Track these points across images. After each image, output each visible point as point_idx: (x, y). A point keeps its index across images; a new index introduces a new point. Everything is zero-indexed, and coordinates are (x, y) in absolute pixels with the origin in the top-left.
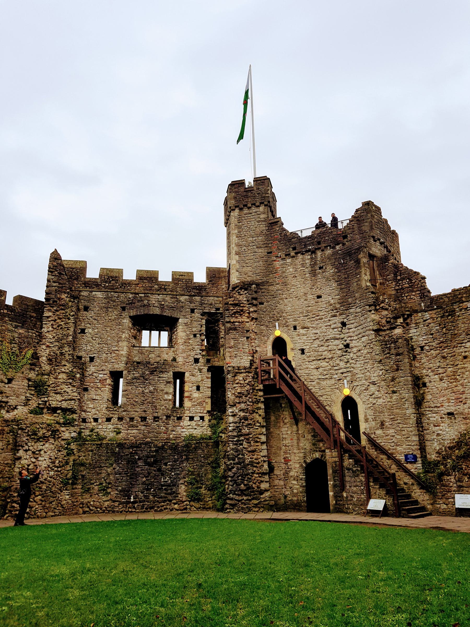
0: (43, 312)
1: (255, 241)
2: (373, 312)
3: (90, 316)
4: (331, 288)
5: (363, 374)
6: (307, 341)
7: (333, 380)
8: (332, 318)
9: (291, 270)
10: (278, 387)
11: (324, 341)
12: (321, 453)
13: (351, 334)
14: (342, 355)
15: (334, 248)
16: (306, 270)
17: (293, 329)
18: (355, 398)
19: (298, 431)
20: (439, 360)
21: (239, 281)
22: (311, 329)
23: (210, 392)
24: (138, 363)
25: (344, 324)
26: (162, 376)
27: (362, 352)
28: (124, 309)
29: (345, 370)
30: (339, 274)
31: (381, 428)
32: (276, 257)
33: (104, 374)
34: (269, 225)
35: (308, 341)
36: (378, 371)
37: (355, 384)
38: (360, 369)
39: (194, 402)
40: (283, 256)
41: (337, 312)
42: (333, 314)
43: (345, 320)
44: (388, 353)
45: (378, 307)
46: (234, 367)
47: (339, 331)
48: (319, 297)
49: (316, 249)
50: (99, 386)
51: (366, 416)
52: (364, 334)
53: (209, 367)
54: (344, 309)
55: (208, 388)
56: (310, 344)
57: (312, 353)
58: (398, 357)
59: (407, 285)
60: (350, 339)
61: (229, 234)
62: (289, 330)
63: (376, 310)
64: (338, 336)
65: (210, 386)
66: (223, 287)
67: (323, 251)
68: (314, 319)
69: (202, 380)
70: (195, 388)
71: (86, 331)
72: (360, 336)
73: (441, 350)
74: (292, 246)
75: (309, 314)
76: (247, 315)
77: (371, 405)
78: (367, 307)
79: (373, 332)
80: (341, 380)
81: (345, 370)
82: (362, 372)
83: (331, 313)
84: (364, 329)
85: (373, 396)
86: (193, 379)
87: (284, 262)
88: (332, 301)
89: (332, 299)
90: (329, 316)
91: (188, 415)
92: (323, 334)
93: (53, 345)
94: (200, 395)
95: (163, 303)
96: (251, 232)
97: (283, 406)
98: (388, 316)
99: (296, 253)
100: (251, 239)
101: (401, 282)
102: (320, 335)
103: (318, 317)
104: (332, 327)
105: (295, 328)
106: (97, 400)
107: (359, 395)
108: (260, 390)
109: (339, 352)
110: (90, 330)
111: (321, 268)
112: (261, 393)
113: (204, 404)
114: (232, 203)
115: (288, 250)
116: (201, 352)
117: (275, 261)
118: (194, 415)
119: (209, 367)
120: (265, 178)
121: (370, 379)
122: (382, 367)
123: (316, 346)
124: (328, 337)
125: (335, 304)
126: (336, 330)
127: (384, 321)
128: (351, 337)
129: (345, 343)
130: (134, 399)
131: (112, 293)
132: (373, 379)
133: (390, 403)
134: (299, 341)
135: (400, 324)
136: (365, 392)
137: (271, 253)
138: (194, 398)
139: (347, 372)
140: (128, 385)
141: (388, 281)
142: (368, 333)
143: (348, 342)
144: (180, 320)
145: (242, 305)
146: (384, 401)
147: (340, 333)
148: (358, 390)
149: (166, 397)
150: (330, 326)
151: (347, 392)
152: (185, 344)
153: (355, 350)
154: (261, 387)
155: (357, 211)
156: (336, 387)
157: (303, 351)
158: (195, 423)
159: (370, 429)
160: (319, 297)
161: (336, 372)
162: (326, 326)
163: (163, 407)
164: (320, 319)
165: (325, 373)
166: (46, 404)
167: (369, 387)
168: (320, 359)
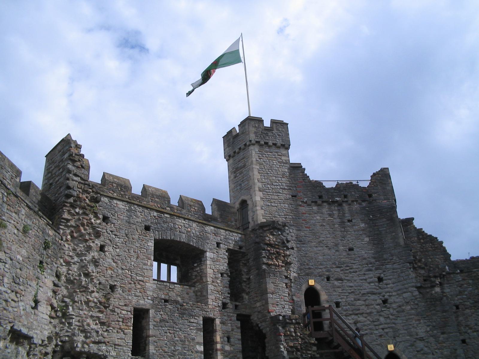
1: (278, 181)
2: (412, 269)
3: (111, 229)
4: (363, 243)
5: (406, 330)
6: (342, 294)
7: (374, 335)
8: (367, 273)
9: (318, 217)
11: (360, 295)
14: (382, 311)
15: (360, 204)
16: (335, 220)
17: (326, 280)
20: (476, 318)
21: (265, 220)
23: (241, 346)
24: (166, 301)
25: (380, 280)
26: (192, 320)
27: (404, 308)
28: (147, 228)
29: (386, 326)
32: (302, 202)
33: (127, 311)
34: (291, 168)
36: (426, 327)
37: (398, 339)
38: (402, 325)
41: (372, 267)
42: (368, 268)
43: (382, 275)
44: (434, 310)
46: (284, 316)
47: (377, 286)
49: (343, 201)
50: (122, 327)
52: (405, 290)
54: (379, 264)
55: (239, 340)
56: (345, 297)
57: (349, 307)
58: (444, 314)
60: (388, 294)
62: (323, 280)
63: (414, 268)
64: (375, 291)
65: (240, 337)
68: (347, 272)
69: (233, 330)
70: (226, 339)
71: (106, 249)
73: (476, 309)
74: (319, 194)
76: (282, 258)
78: (408, 264)
80: (383, 336)
81: (386, 325)
82: (405, 328)
83: (366, 266)
84: (406, 286)
85: (422, 352)
87: (311, 208)
88: (366, 255)
89: (366, 253)
90: (364, 269)
92: (359, 288)
93: (72, 261)
94: (232, 349)
95: (189, 229)
96: (274, 171)
98: (425, 275)
99: (323, 202)
100: (274, 178)
101: (425, 245)
102: (356, 288)
103: (352, 270)
104: (368, 280)
105: (328, 279)
106: (120, 346)
108: (314, 344)
109: (378, 307)
110: (111, 249)
111: (349, 221)
112: (315, 348)
115: (314, 197)
117: (300, 206)
120: (282, 122)
121: (417, 335)
122: (429, 323)
123: (352, 299)
126: (372, 284)
127: (422, 279)
128: (389, 292)
129: (383, 299)
130: (164, 348)
131: (136, 206)
135: (438, 283)
136: (409, 348)
137: (295, 196)
139: (389, 327)
142: (410, 289)
143: (386, 297)
144: (208, 254)
145: (277, 247)
147: (378, 288)
150: (366, 280)
151: (391, 347)
152: (213, 284)
153: (394, 305)
154: (313, 341)
156: (378, 343)
160: (351, 249)
161: (377, 327)
162: (361, 280)
164: (354, 272)
167: (415, 343)
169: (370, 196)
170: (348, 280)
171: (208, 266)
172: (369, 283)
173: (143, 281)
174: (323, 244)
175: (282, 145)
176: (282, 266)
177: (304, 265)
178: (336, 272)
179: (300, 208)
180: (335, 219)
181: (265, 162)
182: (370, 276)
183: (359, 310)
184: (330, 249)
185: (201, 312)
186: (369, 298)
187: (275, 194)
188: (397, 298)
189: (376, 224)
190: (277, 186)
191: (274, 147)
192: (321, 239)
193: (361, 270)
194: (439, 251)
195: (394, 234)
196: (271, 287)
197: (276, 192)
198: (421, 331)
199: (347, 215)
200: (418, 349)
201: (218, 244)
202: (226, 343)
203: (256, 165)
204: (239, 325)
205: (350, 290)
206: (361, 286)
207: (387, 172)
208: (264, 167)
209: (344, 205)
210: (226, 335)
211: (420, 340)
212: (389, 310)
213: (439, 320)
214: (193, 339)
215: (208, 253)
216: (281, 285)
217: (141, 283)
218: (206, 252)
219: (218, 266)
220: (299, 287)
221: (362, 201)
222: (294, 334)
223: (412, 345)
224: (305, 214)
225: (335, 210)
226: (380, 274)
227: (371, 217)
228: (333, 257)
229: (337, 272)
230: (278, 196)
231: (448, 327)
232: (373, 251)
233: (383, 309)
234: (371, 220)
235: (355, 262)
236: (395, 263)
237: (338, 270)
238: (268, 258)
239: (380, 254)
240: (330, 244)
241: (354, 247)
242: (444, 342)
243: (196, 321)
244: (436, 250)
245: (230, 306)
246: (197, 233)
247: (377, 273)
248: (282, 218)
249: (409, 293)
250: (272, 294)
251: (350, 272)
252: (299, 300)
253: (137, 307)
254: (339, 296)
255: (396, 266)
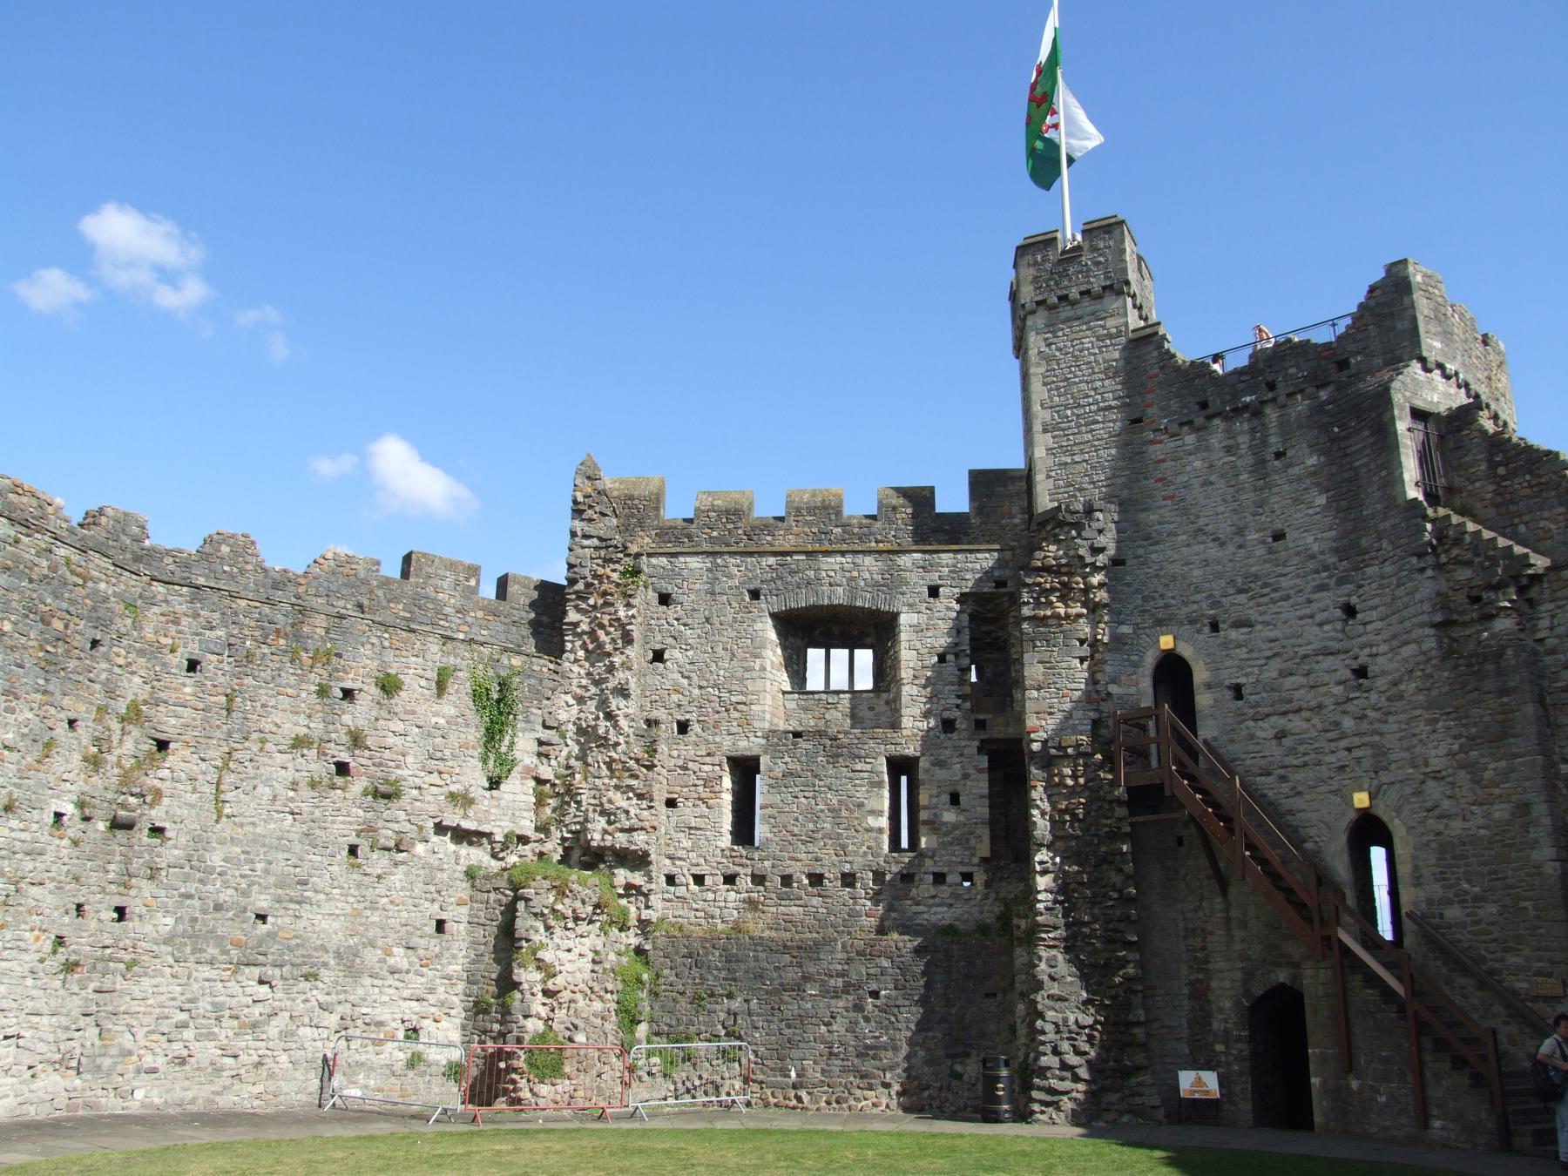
0: (565, 613)
1: (1093, 393)
2: (1430, 573)
4: (1311, 511)
5: (1407, 749)
8: (1316, 596)
9: (1198, 464)
10: (1167, 793)
11: (1297, 661)
12: (1291, 971)
13: (1371, 637)
14: (1349, 700)
17: (1207, 629)
18: (1385, 819)
19: (1227, 910)
22: (1259, 627)
24: (797, 735)
25: (1350, 611)
26: (858, 767)
29: (1356, 741)
30: (1334, 469)
31: (1459, 902)
35: (1253, 663)
36: (1450, 741)
37: (1384, 777)
39: (945, 835)
40: (1174, 428)
41: (1330, 577)
43: (1354, 600)
44: (1477, 689)
45: (1443, 559)
47: (1338, 631)
48: (1279, 536)
49: (1263, 403)
51: (1416, 868)
52: (1405, 636)
53: (982, 742)
55: (981, 797)
56: (1256, 670)
57: (1264, 695)
58: (1505, 700)
59: (1528, 491)
60: (1367, 651)
61: (1025, 377)
62: (1198, 631)
63: (1439, 567)
64: (1335, 645)
65: (986, 791)
66: (1017, 521)
67: (1283, 407)
68: (1265, 600)
69: (966, 776)
70: (946, 798)
71: (666, 656)
72: (1395, 643)
75: (1253, 586)
77: (1432, 837)
78: (1414, 560)
79: (1432, 631)
80: (1348, 770)
82: (1405, 744)
83: (1313, 579)
84: (1407, 624)
85: (1436, 812)
86: (940, 774)
87: (1180, 443)
88: (1315, 548)
91: (931, 870)
93: (588, 694)
94: (961, 818)
95: (855, 574)
97: (1186, 841)
99: (1209, 418)
100: (1084, 386)
101: (1508, 483)
102: (1285, 642)
103: (1276, 595)
104: (1318, 619)
105: (1215, 627)
107: (1398, 810)
108: (1119, 802)
109: (1338, 690)
111: (1279, 455)
112: (1121, 812)
113: (973, 842)
114: (1028, 294)
115: (1185, 411)
116: (959, 701)
117: (1152, 442)
118: (945, 870)
119: (982, 742)
120: (1113, 220)
121: (1427, 765)
123: (1274, 674)
124: (1308, 650)
125: (1322, 553)
126: (1327, 627)
127: (1460, 597)
128: (1371, 646)
130: (790, 828)
132: (1436, 763)
133: (1482, 832)
134: (1228, 664)
136: (1413, 799)
137: (1139, 420)
138: (945, 824)
139: (1364, 745)
140: (772, 790)
141: (1472, 483)
146: (1467, 825)
147: (1340, 636)
148: (1392, 795)
149: (872, 821)
150: (1311, 616)
151: (1361, 799)
152: (916, 682)
153: (1381, 683)
155: (1372, 289)
156: (1333, 788)
157: (1238, 691)
158: (949, 890)
159: (1429, 902)
160: (1279, 536)
162: (1301, 618)
163: (864, 848)
165: (1301, 749)
166: (578, 839)
167: (1424, 787)
168: (1285, 713)
169: (1343, 365)
170: (1267, 624)
171: (904, 645)
172: (1321, 625)
173: (745, 704)
174: (1205, 534)
175: (1104, 288)
176: (1079, 616)
177: (1154, 599)
178: (1234, 604)
179: (1151, 448)
180: (1241, 457)
181: (1060, 350)
182: (1321, 605)
183: (1291, 701)
184: (1222, 544)
185: (882, 747)
186: (1317, 667)
187: (1084, 428)
188: (1391, 660)
189: (1348, 451)
190: (1089, 405)
191: (1086, 302)
192: (1201, 522)
193: (1300, 591)
194: (1553, 493)
195: (1383, 473)
196: (1033, 670)
197: (1086, 424)
198: (1437, 756)
199: (1272, 439)
200: (1428, 805)
201: (934, 592)
202: (948, 806)
203: (1038, 365)
204: (986, 765)
205: (1271, 649)
206: (1301, 636)
207: (1402, 274)
208: (1058, 364)
209: (1268, 410)
210: (951, 789)
211: (1435, 778)
212: (1366, 695)
213: (1488, 718)
214: (861, 805)
215: (902, 616)
216: (1064, 665)
217: (740, 707)
218: (898, 614)
219: (929, 640)
220: (1136, 658)
221: (1318, 387)
222: (1070, 782)
223: (1418, 793)
224: (1163, 461)
225: (1243, 432)
226: (1349, 595)
227: (1336, 430)
228: (1231, 564)
229: (1241, 605)
230: (1092, 431)
231: (1512, 740)
232: (1334, 533)
233: (1351, 696)
234: (1335, 440)
235: (1287, 570)
236: (1385, 560)
237: (1242, 598)
238: (1038, 604)
239: (1353, 537)
240: (1225, 530)
241: (1287, 530)
242: (1497, 785)
243: (869, 767)
244: (1544, 494)
245: (961, 725)
246: (875, 576)
247: (1343, 593)
248: (1099, 487)
249: (1413, 646)
250: (1039, 688)
251: (1273, 602)
252: (1132, 690)
253: (733, 754)
254: (1240, 668)
255: (1389, 568)
